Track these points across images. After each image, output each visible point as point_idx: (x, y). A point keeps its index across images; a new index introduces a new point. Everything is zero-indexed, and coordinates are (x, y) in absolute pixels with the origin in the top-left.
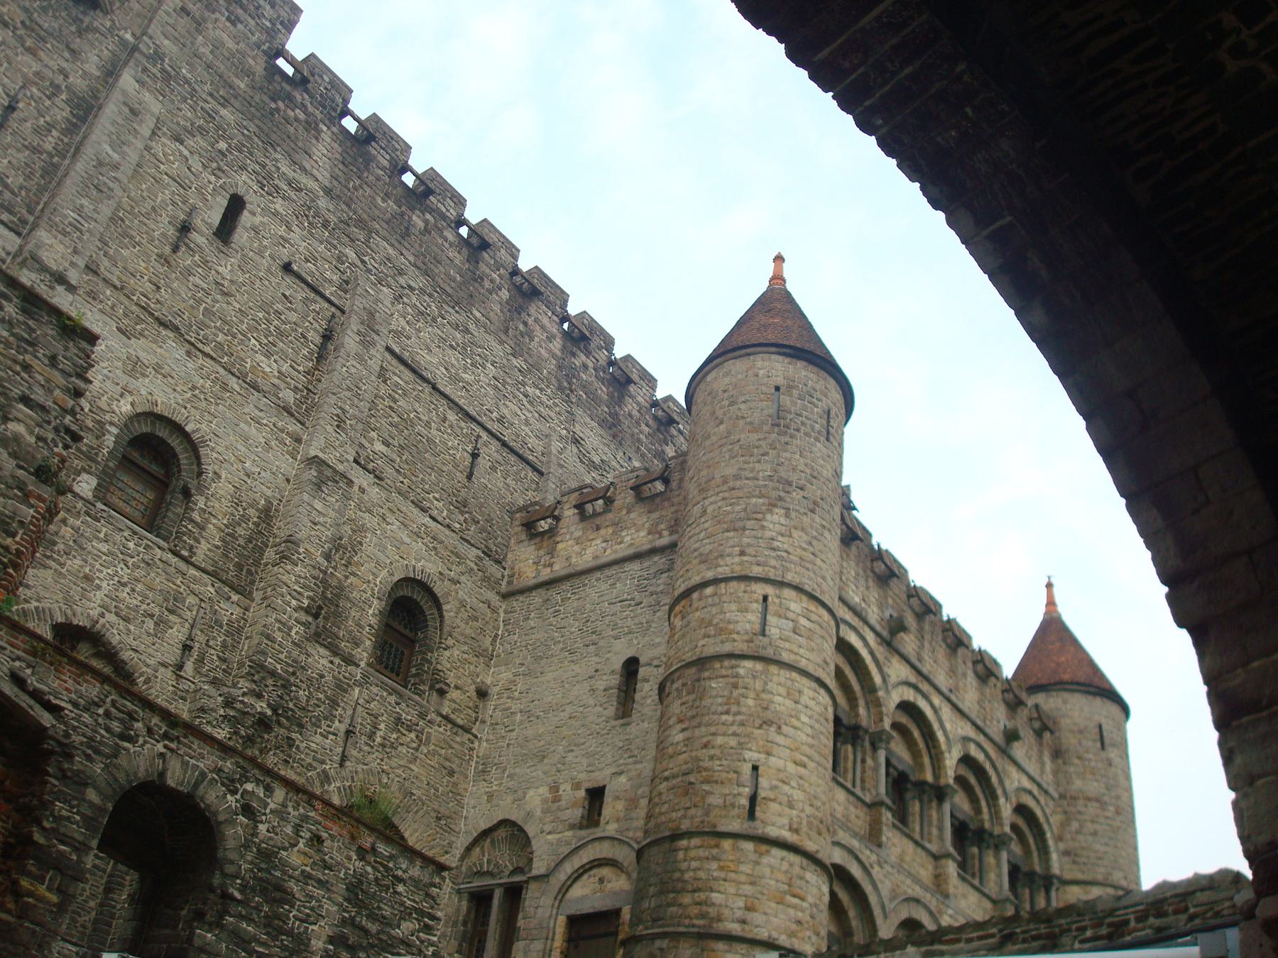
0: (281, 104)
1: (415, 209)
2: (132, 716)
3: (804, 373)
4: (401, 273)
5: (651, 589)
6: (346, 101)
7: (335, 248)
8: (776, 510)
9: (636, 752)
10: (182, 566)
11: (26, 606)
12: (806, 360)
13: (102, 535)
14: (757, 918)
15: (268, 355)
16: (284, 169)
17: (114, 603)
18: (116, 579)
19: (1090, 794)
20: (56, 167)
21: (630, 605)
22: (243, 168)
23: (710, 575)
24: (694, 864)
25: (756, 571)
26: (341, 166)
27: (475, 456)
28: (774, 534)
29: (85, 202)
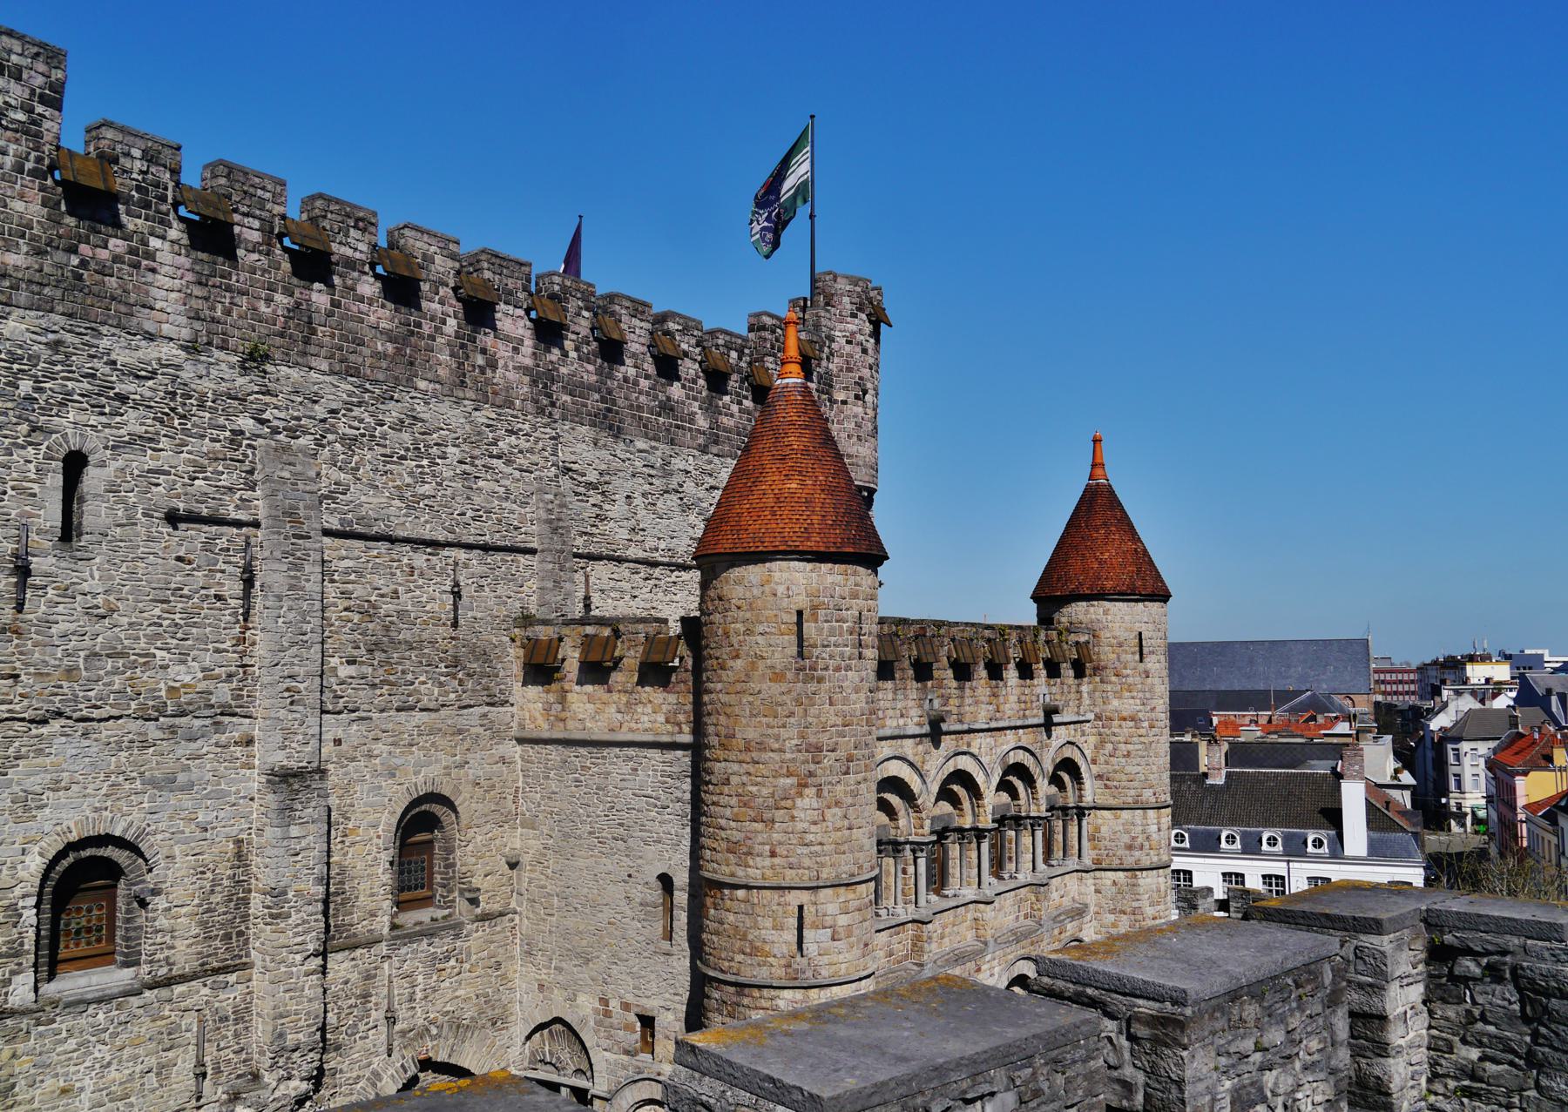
0: (84, 249)
3: (830, 579)
8: (807, 791)
16: (122, 357)
18: (97, 1066)
19: (1125, 714)
25: (790, 877)
26: (197, 291)
28: (806, 825)
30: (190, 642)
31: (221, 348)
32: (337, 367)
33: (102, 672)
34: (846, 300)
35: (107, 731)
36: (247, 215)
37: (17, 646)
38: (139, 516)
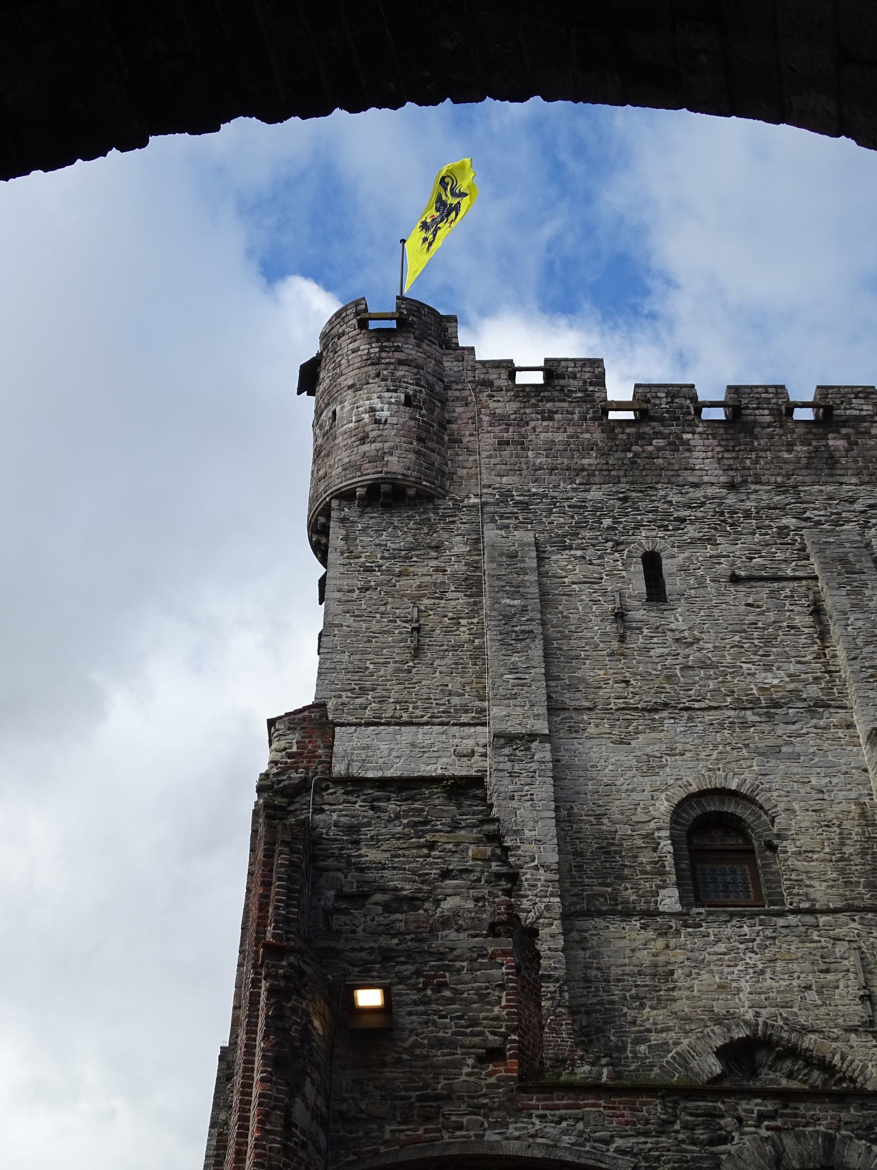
0: (634, 448)
1: (826, 435)
2: (713, 1115)
4: (852, 501)
6: (694, 398)
7: (770, 527)
10: (809, 919)
11: (679, 1049)
15: (768, 668)
17: (763, 997)
18: (751, 971)
20: (480, 647)
22: (638, 526)
26: (726, 455)
29: (515, 658)
30: (772, 657)
31: (756, 483)
32: (867, 479)
33: (697, 678)
36: (758, 408)
37: (624, 663)
38: (708, 581)
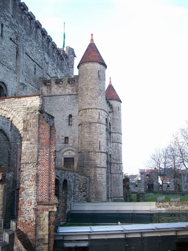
3: (102, 67)
5: (73, 102)
8: (100, 96)
9: (73, 132)
12: (103, 65)
13: (53, 146)
14: (101, 164)
21: (69, 104)
23: (90, 107)
24: (93, 157)
27: (35, 69)
34: (71, 51)
35: (5, 67)
